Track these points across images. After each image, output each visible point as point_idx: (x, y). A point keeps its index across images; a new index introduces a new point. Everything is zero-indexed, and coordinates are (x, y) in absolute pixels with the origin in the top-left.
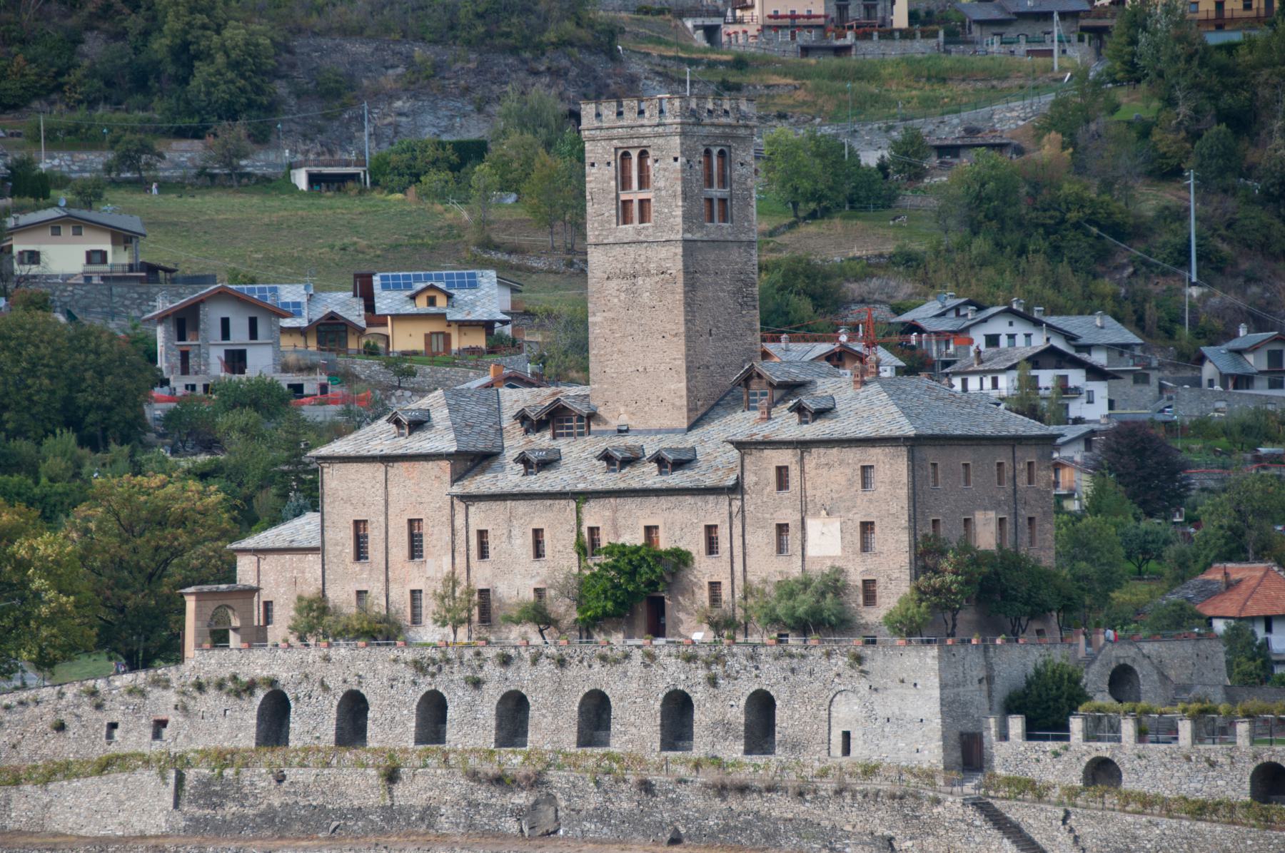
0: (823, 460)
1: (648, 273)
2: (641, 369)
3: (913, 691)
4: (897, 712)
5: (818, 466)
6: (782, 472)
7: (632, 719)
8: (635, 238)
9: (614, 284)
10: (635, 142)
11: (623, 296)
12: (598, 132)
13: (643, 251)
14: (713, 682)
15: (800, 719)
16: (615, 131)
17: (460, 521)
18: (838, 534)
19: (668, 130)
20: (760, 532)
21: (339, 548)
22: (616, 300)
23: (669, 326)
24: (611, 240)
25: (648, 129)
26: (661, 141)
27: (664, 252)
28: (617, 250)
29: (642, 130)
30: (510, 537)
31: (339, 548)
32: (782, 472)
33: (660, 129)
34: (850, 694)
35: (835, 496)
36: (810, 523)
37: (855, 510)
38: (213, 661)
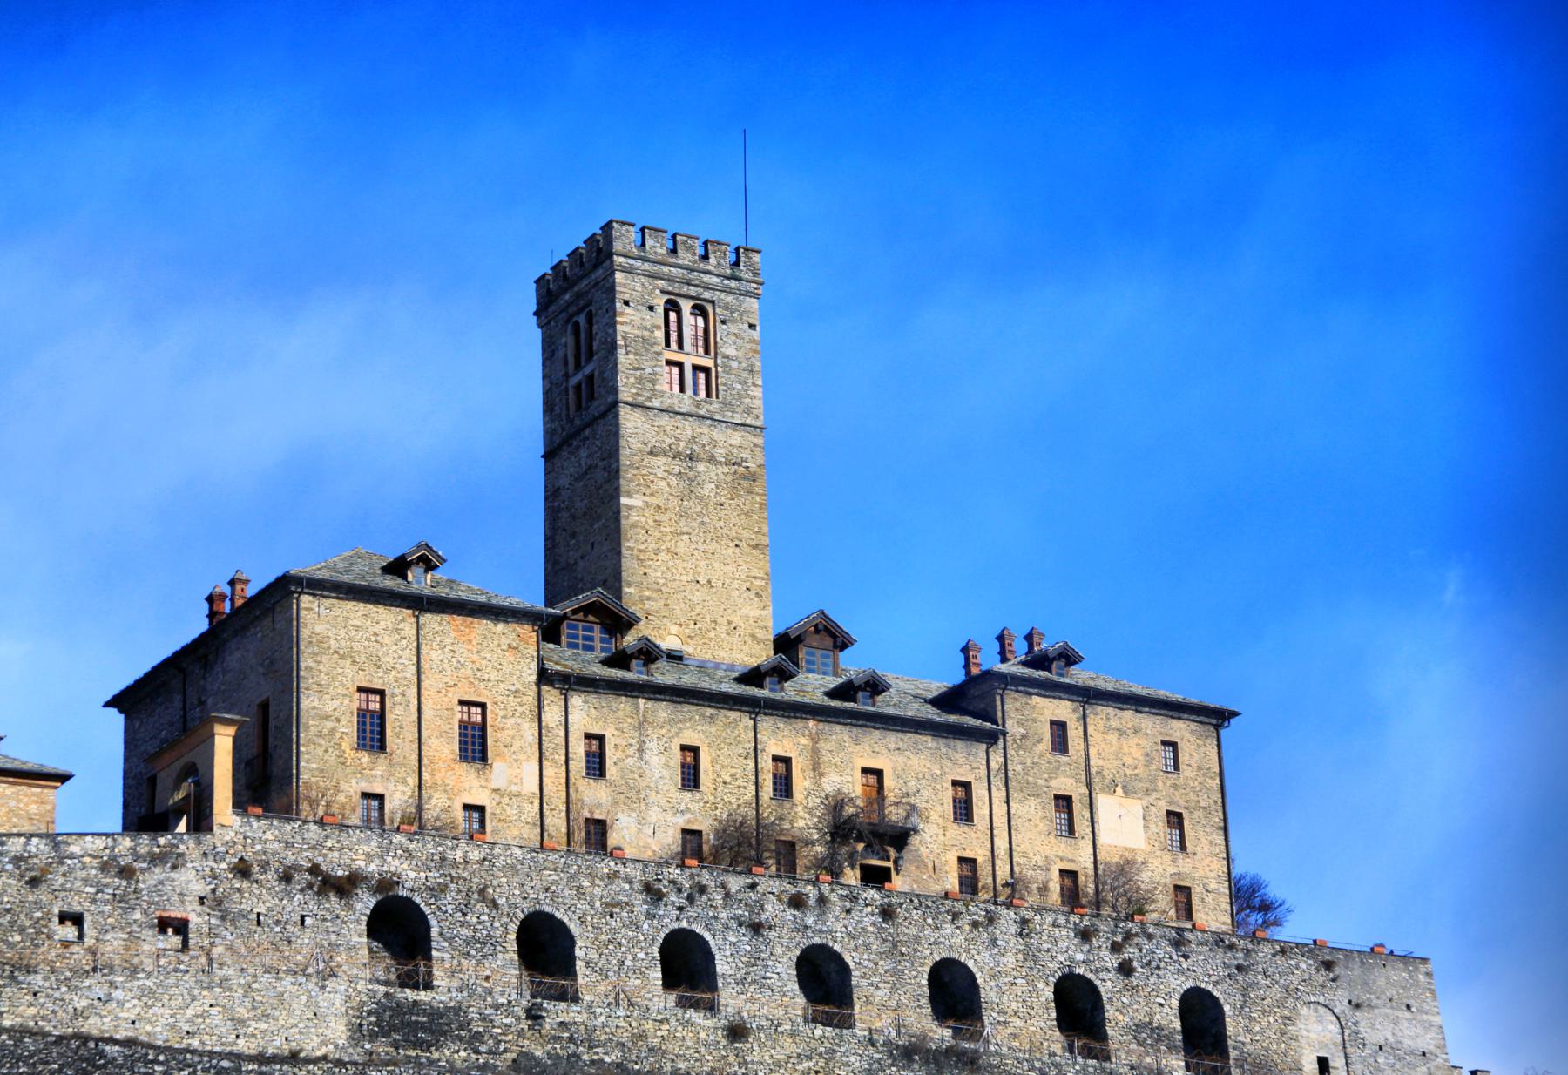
0: (1114, 724)
1: (712, 460)
2: (703, 581)
3: (1408, 1015)
4: (1392, 1040)
5: (1108, 729)
6: (1059, 728)
7: (1014, 1006)
8: (694, 410)
9: (660, 461)
10: (692, 291)
11: (674, 482)
12: (638, 264)
13: (706, 432)
14: (1125, 969)
15: (1262, 1032)
16: (666, 269)
17: (552, 715)
18: (1142, 822)
19: (743, 286)
20: (1033, 802)
21: (329, 725)
22: (663, 484)
23: (745, 534)
24: (656, 403)
25: (715, 280)
26: (730, 298)
27: (736, 438)
28: (664, 420)
29: (706, 278)
30: (641, 750)
31: (329, 725)
32: (1059, 728)
33: (733, 284)
34: (1322, 1010)
35: (1129, 772)
36: (1102, 801)
37: (1155, 795)
38: (269, 835)
